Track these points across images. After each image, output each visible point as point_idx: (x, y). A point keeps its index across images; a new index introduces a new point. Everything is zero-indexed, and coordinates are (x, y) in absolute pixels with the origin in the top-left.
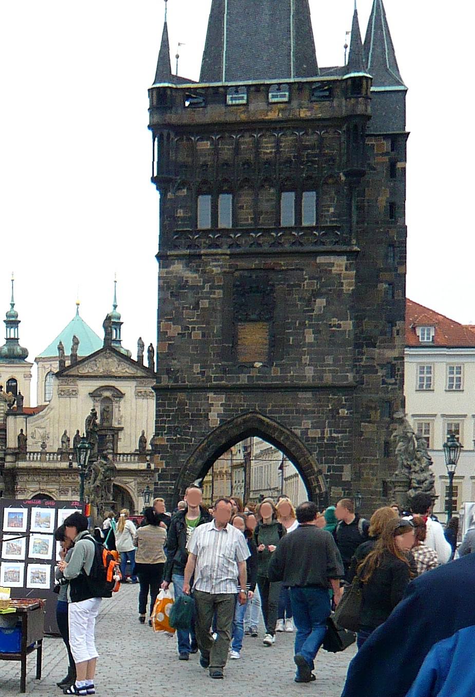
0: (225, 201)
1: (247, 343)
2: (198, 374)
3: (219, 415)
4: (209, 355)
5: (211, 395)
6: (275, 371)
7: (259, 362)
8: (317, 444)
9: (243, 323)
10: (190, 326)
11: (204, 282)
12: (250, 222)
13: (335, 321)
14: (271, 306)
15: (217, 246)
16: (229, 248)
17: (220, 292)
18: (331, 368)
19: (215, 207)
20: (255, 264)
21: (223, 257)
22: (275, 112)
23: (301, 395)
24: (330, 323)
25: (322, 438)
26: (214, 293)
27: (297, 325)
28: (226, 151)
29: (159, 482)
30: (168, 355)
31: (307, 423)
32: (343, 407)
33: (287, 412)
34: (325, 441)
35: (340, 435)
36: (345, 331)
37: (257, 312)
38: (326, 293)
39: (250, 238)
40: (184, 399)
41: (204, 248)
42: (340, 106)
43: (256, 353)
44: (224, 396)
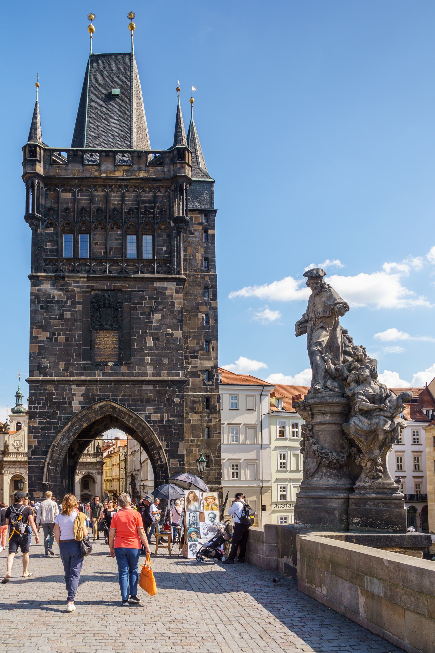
0: (83, 240)
2: (63, 370)
3: (80, 403)
5: (74, 387)
6: (124, 369)
7: (112, 362)
8: (158, 426)
10: (57, 332)
12: (103, 255)
13: (169, 331)
15: (78, 272)
16: (86, 273)
17: (80, 307)
19: (75, 242)
21: (82, 279)
22: (120, 172)
23: (144, 387)
25: (162, 421)
26: (75, 307)
28: (84, 201)
29: (33, 457)
30: (39, 354)
31: (150, 409)
32: (177, 396)
33: (134, 400)
34: (164, 423)
35: (175, 418)
36: (177, 338)
37: (109, 323)
38: (162, 310)
39: (103, 266)
40: (52, 390)
41: (68, 273)
42: (169, 171)
43: (109, 355)
44: (84, 388)
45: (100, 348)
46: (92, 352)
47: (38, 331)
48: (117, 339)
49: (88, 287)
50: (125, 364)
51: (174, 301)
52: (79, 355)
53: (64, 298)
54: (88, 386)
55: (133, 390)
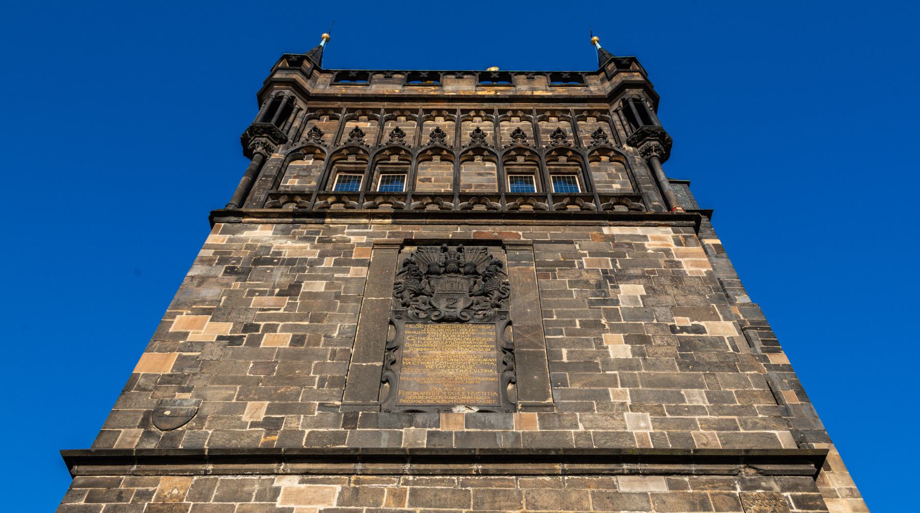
1: (429, 365)
2: (253, 425)
4: (304, 382)
5: (289, 483)
9: (420, 326)
10: (262, 324)
11: (322, 255)
14: (496, 294)
18: (708, 417)
20: (454, 234)
23: (625, 484)
24: (669, 324)
27: (578, 327)
37: (461, 305)
40: (177, 496)
44: (338, 488)
45: (424, 367)
46: (388, 373)
47: (195, 321)
48: (489, 343)
49: (393, 234)
50: (526, 408)
51: (676, 259)
52: (334, 382)
53: (314, 254)
54: (357, 482)
55: (574, 496)
